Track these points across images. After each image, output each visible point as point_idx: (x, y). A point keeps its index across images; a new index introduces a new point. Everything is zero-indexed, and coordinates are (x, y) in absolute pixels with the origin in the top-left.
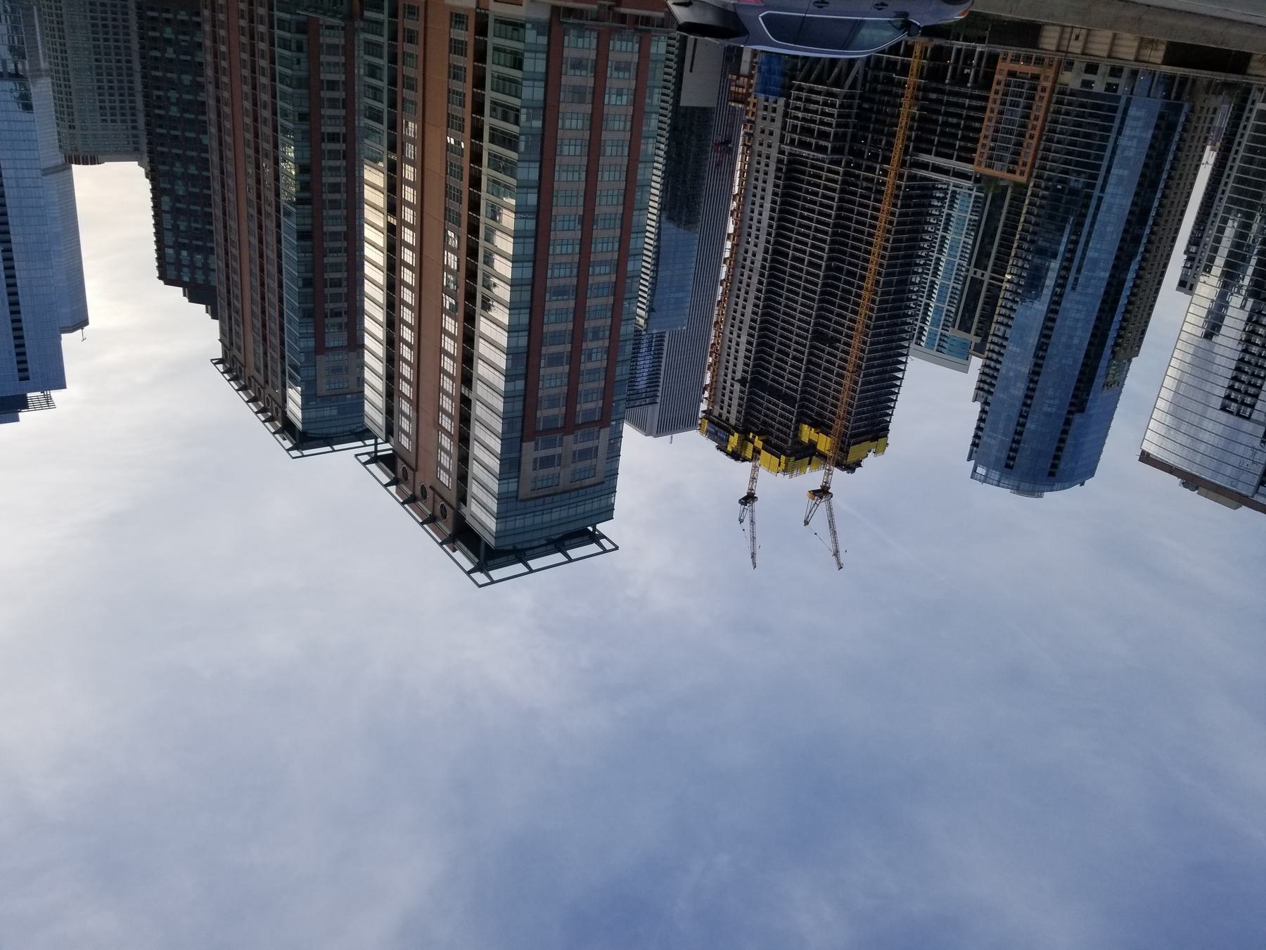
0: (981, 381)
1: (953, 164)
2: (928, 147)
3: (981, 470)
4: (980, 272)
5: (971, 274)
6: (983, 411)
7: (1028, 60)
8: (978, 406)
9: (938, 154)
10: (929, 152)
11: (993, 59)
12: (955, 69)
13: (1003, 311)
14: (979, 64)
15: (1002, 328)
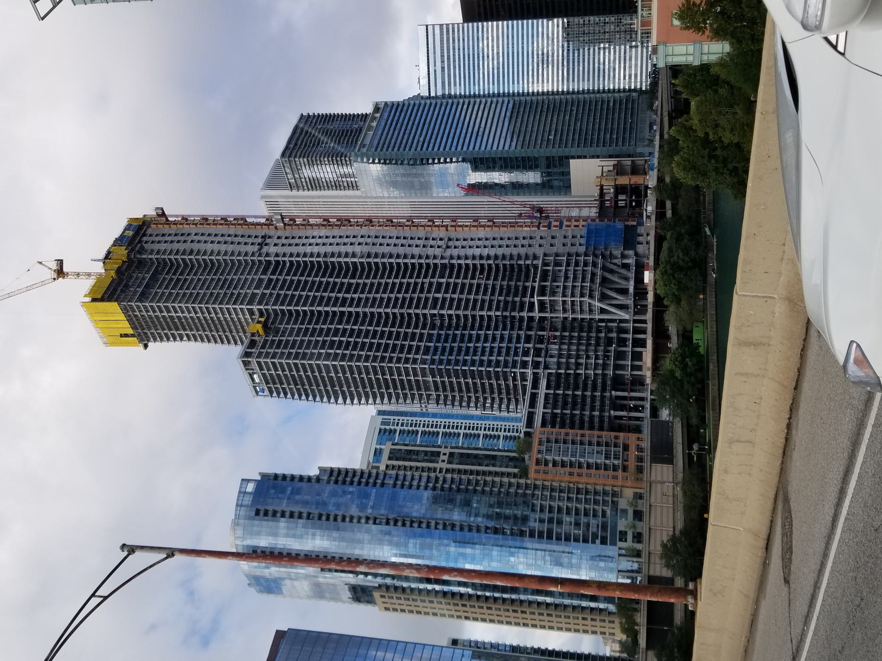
0: (339, 471)
1: (540, 410)
2: (553, 384)
3: (250, 487)
4: (446, 458)
5: (443, 450)
6: (309, 479)
7: (640, 459)
8: (314, 472)
9: (547, 395)
10: (548, 387)
11: (638, 430)
12: (624, 398)
13: (409, 478)
14: (630, 418)
15: (392, 482)
